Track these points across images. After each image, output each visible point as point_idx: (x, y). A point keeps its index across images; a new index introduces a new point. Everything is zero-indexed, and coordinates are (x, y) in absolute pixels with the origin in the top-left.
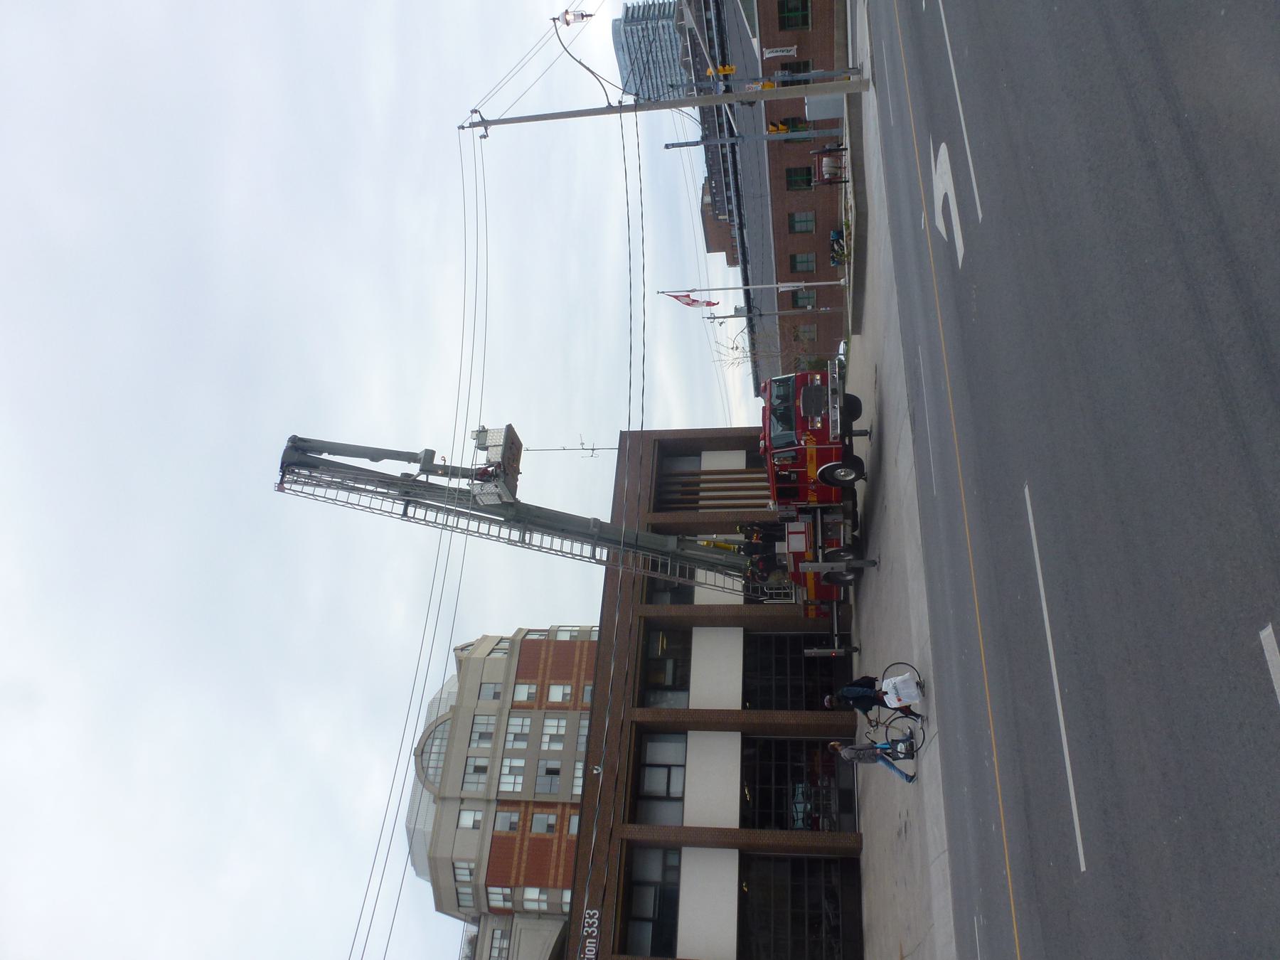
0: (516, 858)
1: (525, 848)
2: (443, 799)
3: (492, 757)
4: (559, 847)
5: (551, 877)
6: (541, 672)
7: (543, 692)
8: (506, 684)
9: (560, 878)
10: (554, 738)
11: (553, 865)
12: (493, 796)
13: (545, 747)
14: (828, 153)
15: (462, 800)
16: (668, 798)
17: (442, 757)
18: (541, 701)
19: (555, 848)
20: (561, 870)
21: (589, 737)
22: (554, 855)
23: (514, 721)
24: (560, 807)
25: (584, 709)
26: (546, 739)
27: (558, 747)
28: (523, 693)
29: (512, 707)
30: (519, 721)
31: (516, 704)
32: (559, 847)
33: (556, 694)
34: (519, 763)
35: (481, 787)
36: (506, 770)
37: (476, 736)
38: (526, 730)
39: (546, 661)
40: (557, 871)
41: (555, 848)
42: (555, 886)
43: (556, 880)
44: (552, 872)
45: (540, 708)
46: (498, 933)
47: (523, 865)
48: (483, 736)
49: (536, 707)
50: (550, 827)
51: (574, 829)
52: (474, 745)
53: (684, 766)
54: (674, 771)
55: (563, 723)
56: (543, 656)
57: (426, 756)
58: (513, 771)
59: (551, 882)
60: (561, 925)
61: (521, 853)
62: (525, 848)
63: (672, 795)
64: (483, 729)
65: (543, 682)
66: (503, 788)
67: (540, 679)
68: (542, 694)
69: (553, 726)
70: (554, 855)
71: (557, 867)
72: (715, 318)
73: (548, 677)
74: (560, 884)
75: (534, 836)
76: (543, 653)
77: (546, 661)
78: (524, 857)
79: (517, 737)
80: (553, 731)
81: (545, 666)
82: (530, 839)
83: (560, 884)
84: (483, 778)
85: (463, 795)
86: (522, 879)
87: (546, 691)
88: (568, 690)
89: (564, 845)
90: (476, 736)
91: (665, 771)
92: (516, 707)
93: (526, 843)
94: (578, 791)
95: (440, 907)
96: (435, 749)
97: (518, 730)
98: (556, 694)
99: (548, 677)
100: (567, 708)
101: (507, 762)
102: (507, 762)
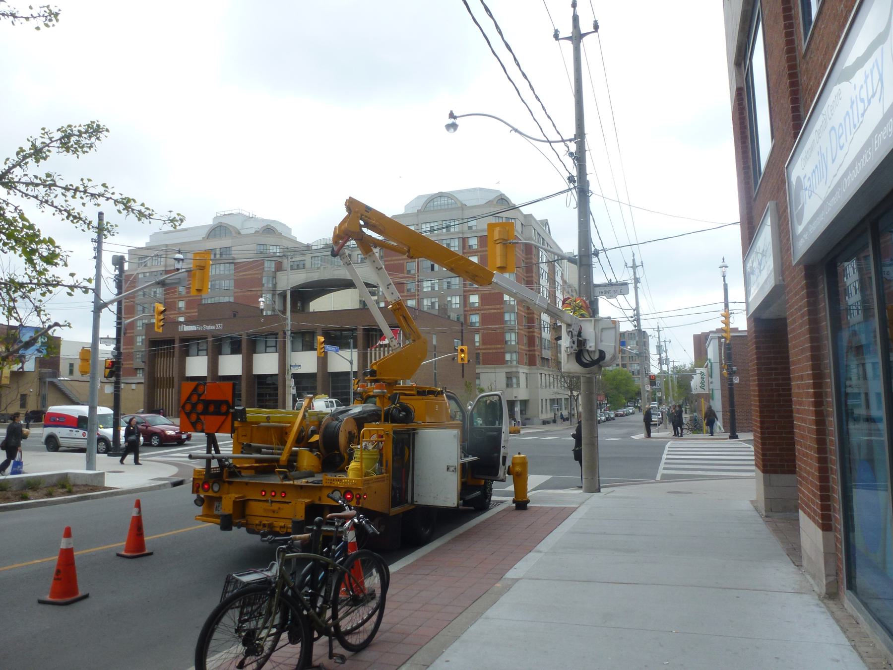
0: (396, 258)
1: (400, 262)
2: (417, 215)
8: (477, 231)
15: (417, 225)
16: (266, 347)
17: (439, 208)
18: (469, 253)
23: (456, 241)
28: (474, 242)
29: (464, 239)
30: (457, 244)
31: (467, 240)
47: (392, 262)
49: (465, 251)
50: (409, 272)
54: (274, 349)
61: (397, 260)
62: (400, 262)
65: (479, 252)
67: (480, 249)
72: (659, 331)
73: (481, 254)
75: (405, 264)
78: (396, 262)
82: (403, 264)
85: (420, 225)
86: (387, 263)
87: (474, 254)
91: (275, 345)
93: (401, 262)
97: (452, 245)
99: (481, 254)
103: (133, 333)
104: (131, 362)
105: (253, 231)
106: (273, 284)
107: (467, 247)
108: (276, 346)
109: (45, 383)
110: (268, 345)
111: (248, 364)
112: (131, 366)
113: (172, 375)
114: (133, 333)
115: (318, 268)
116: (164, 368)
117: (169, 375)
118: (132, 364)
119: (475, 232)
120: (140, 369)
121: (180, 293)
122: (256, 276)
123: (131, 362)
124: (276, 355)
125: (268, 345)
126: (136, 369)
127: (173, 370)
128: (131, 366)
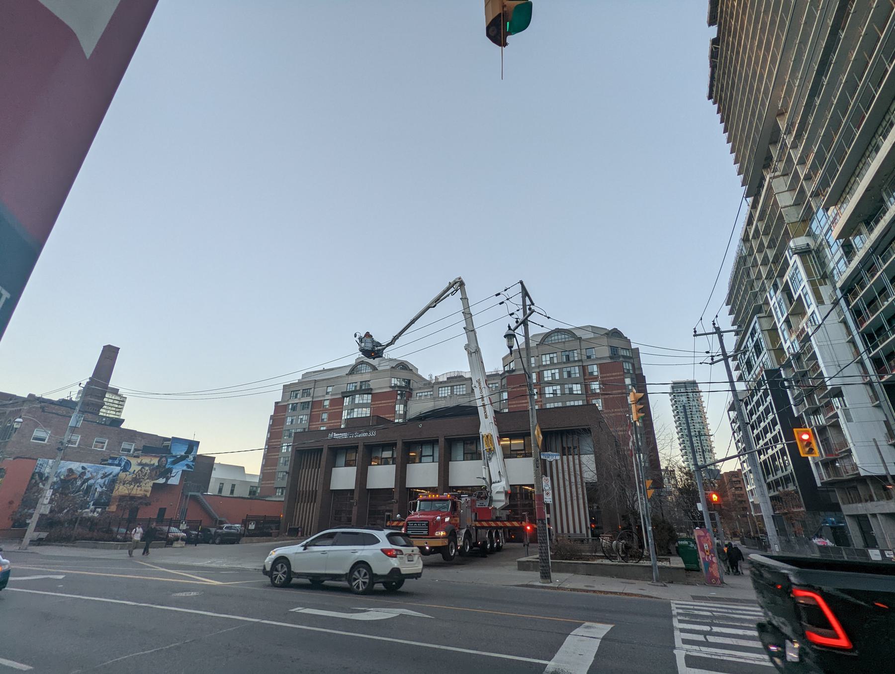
3: (558, 363)
4: (524, 403)
5: (512, 403)
6: (605, 375)
7: (595, 379)
9: (512, 406)
10: (571, 389)
11: (517, 402)
12: (542, 369)
13: (566, 386)
14: (627, 548)
19: (523, 401)
20: (515, 406)
21: (574, 406)
22: (521, 402)
23: (577, 368)
24: (541, 399)
25: (587, 401)
26: (570, 386)
27: (567, 391)
30: (577, 371)
31: (586, 367)
32: (524, 403)
33: (595, 386)
34: (557, 377)
35: (544, 363)
36: (553, 371)
37: (567, 353)
38: (573, 376)
39: (613, 376)
40: (515, 404)
41: (523, 401)
42: (509, 405)
43: (511, 405)
44: (514, 402)
45: (585, 379)
46: (497, 385)
48: (568, 357)
49: (586, 377)
51: (322, 429)
52: (563, 353)
53: (433, 462)
54: (430, 459)
55: (580, 392)
56: (614, 374)
57: (556, 334)
58: (553, 374)
59: (510, 403)
60: (498, 410)
63: (423, 458)
64: (570, 356)
66: (545, 372)
68: (592, 379)
69: (577, 389)
70: (521, 402)
71: (517, 404)
74: (510, 406)
76: (616, 374)
77: (613, 376)
79: (569, 374)
80: (574, 389)
81: (608, 377)
82: (526, 390)
83: (510, 406)
84: (548, 363)
88: (598, 391)
89: (525, 405)
90: (567, 353)
92: (584, 369)
94: (548, 406)
95: (503, 359)
96: (560, 337)
98: (595, 386)
100: (587, 392)
101: (557, 371)
102: (557, 371)
103: (278, 455)
104: (272, 482)
105: (388, 367)
106: (404, 411)
107: (587, 373)
108: (433, 456)
109: (187, 496)
110: (423, 454)
111: (401, 476)
112: (272, 485)
113: (316, 488)
114: (278, 455)
115: (445, 397)
116: (309, 479)
117: (313, 488)
118: (273, 483)
119: (593, 359)
120: (280, 488)
121: (323, 420)
122: (390, 404)
123: (272, 482)
124: (436, 465)
125: (423, 454)
126: (277, 488)
127: (317, 481)
128: (272, 485)
